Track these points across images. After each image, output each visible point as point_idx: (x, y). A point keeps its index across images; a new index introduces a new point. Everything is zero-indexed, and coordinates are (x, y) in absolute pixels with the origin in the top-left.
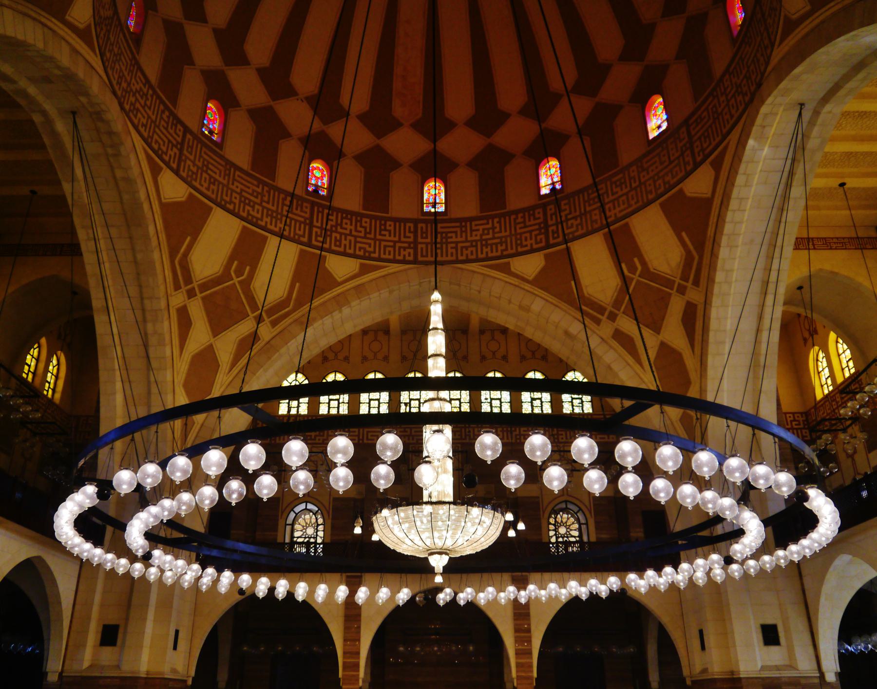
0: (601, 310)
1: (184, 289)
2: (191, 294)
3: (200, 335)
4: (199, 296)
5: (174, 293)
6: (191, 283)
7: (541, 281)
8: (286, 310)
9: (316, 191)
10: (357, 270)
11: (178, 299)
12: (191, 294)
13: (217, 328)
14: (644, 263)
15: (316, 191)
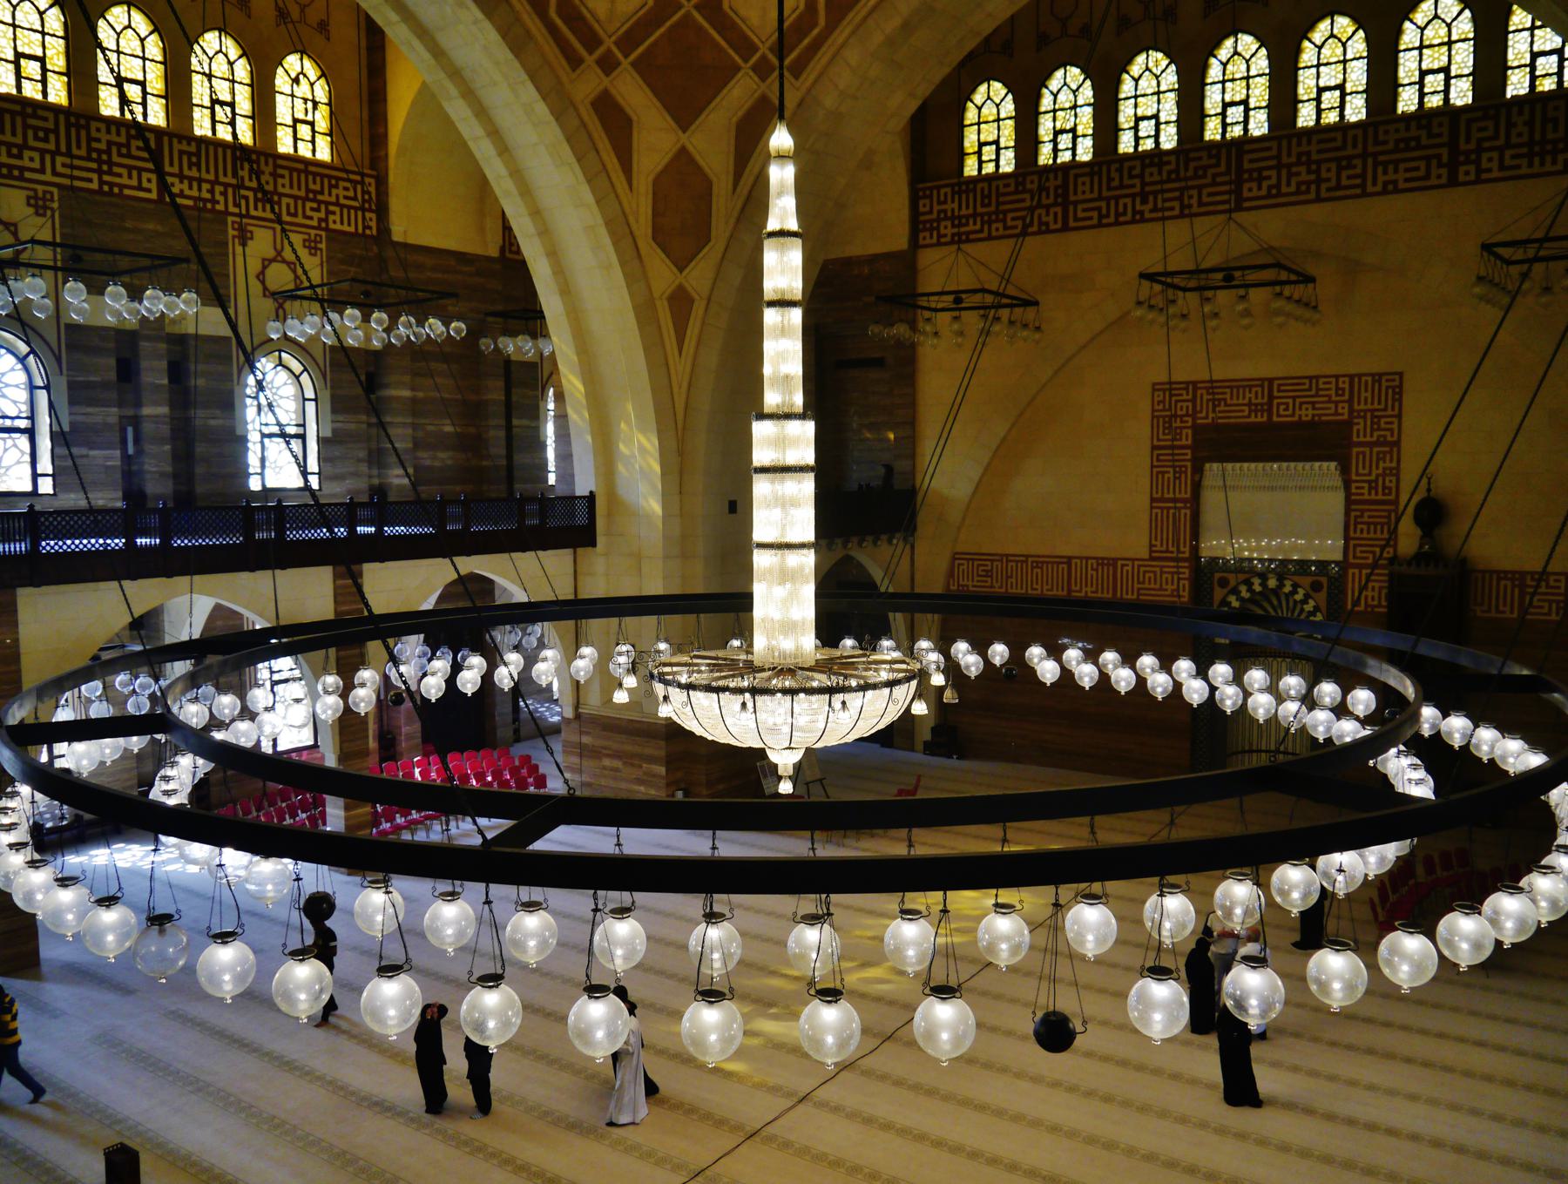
1: (590, 60)
2: (608, 65)
3: (656, 138)
4: (626, 63)
5: (574, 76)
6: (600, 42)
8: (816, 32)
11: (588, 84)
12: (608, 65)
13: (684, 111)
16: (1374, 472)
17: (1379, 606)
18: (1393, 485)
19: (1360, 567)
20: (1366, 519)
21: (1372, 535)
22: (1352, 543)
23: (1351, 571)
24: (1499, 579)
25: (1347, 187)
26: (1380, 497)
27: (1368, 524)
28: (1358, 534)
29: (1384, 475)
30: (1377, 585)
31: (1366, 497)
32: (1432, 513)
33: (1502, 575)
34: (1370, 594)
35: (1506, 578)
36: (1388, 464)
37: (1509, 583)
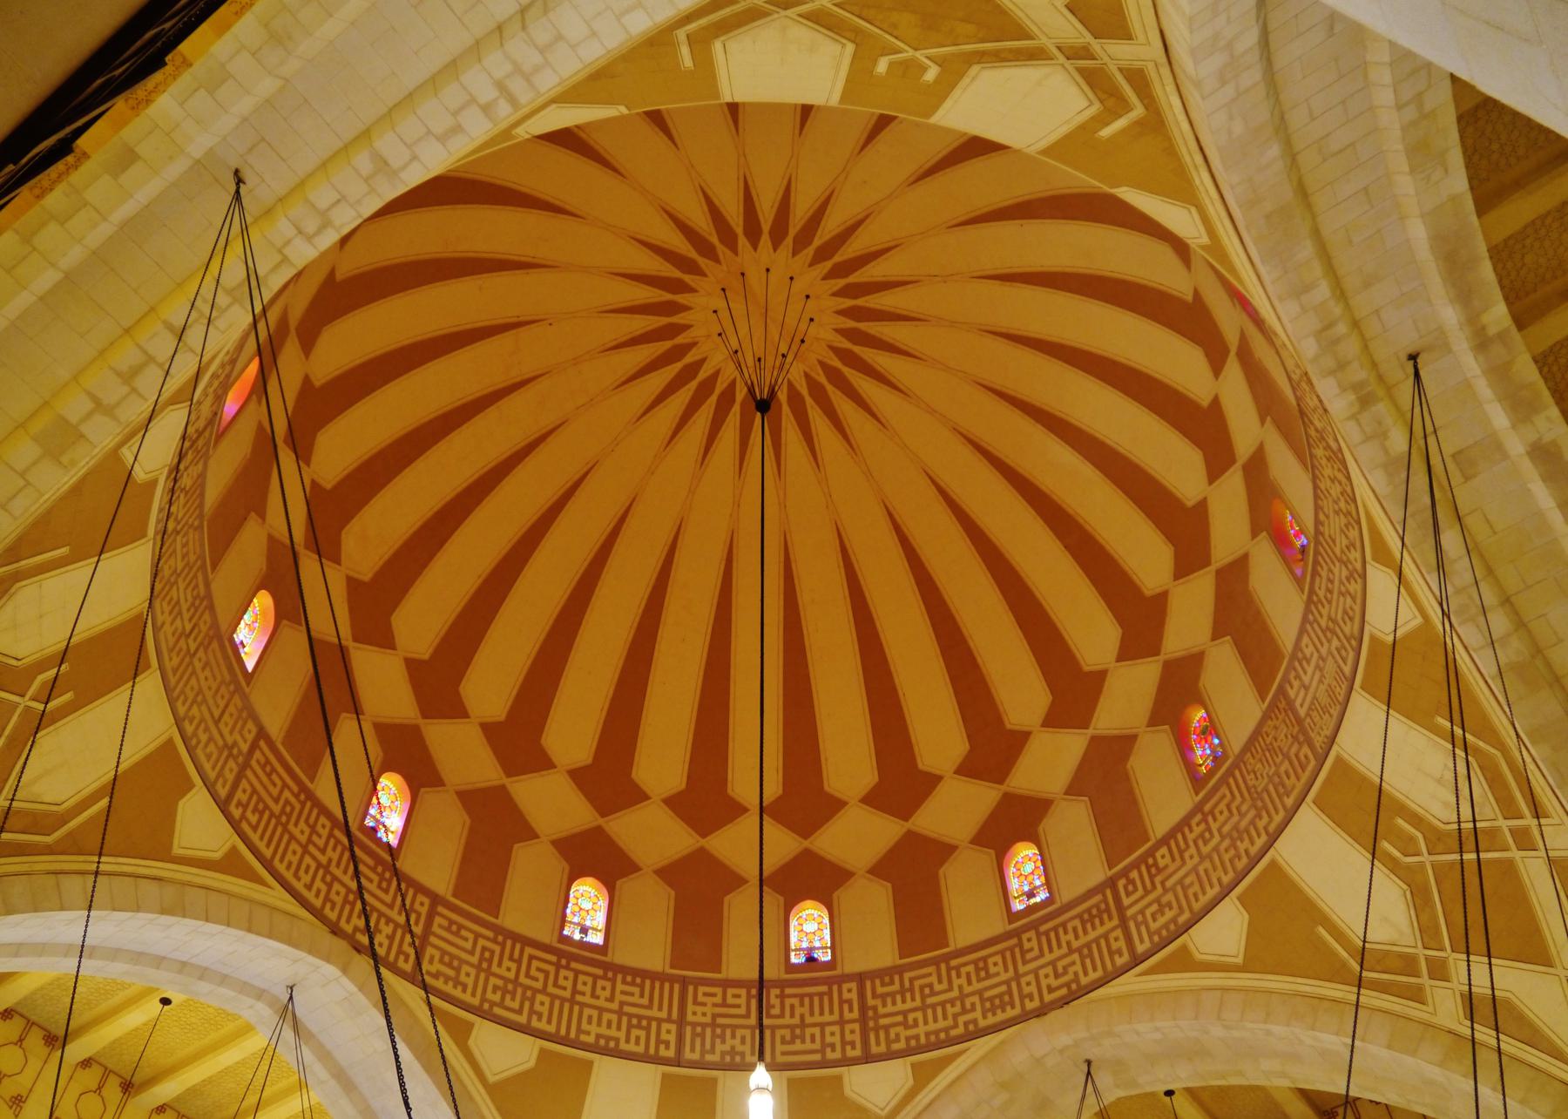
0: (1408, 965)
7: (1261, 954)
9: (811, 959)
10: (911, 1082)
14: (1416, 820)
15: (811, 959)
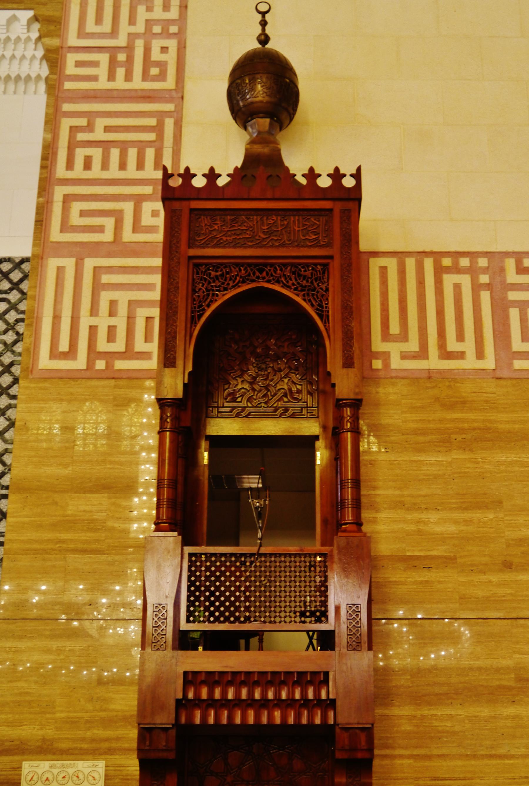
16: (125, 29)
17: (129, 353)
18: (171, 58)
19: (81, 252)
20: (99, 135)
21: (114, 172)
22: (59, 193)
23: (53, 264)
24: (440, 271)
25: (100, 49)
26: (137, 83)
27: (106, 146)
28: (79, 172)
29: (148, 34)
30: (123, 298)
31: (103, 84)
32: (266, 89)
33: (444, 261)
34: (103, 322)
35: (456, 269)
36: (158, 13)
37: (465, 280)
